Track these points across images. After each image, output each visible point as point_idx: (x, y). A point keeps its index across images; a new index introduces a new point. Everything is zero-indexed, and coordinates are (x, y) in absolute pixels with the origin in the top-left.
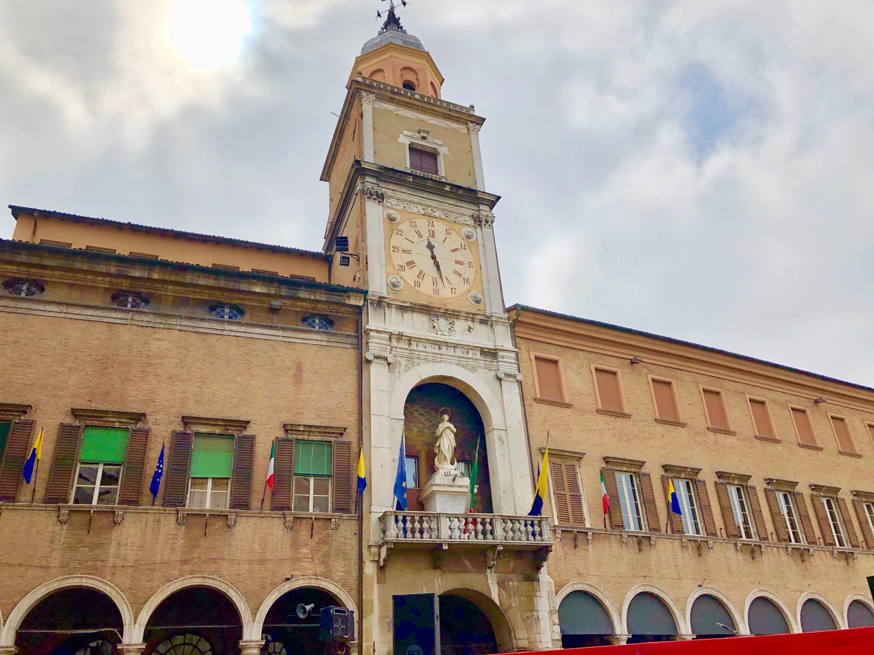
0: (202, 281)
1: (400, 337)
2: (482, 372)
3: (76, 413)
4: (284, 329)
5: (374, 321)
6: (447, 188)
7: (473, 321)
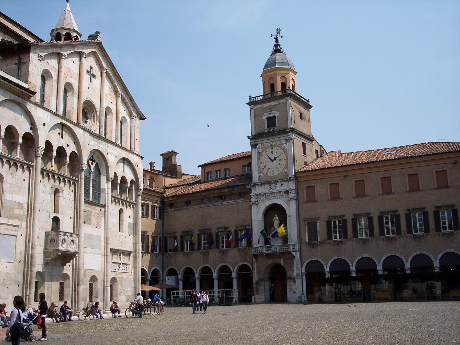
0: (215, 192)
2: (285, 199)
3: (200, 231)
4: (235, 199)
5: (253, 192)
6: (276, 133)
7: (283, 181)
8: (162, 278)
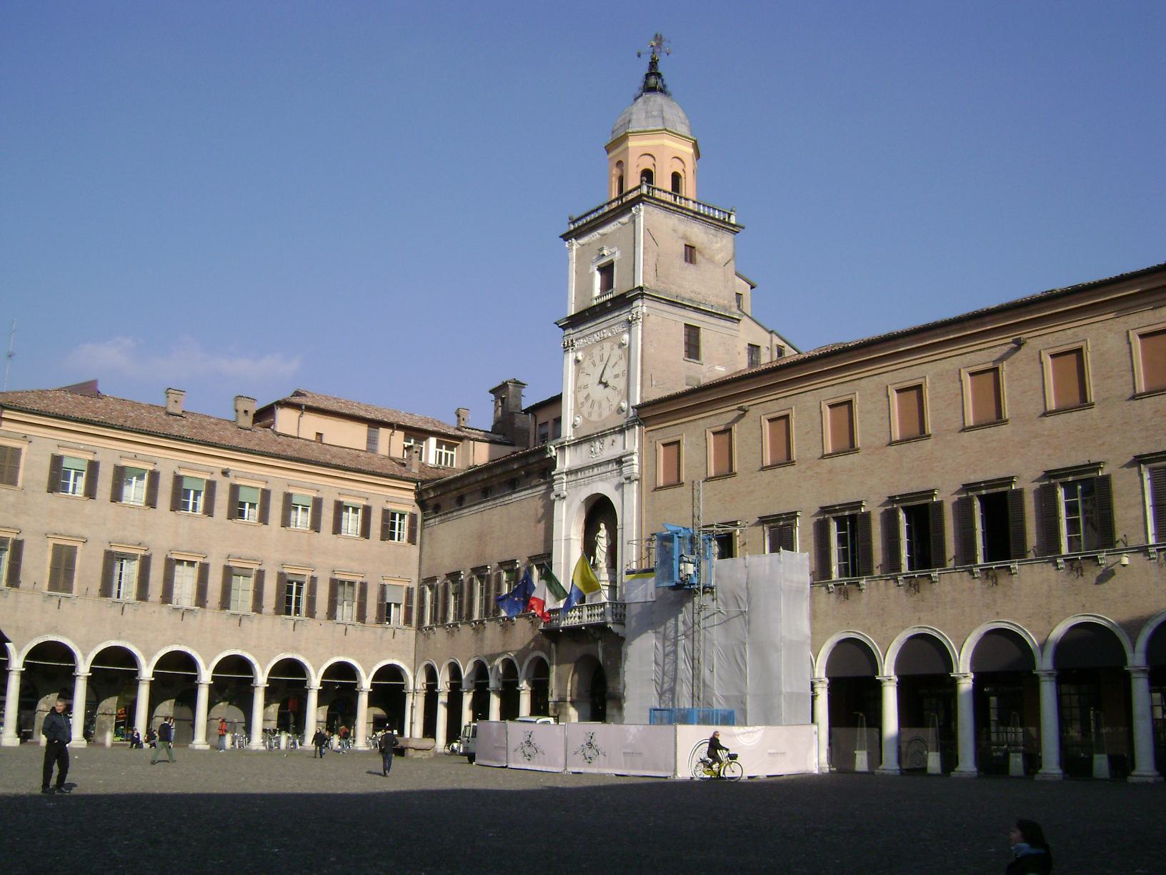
0: (499, 471)
8: (411, 687)
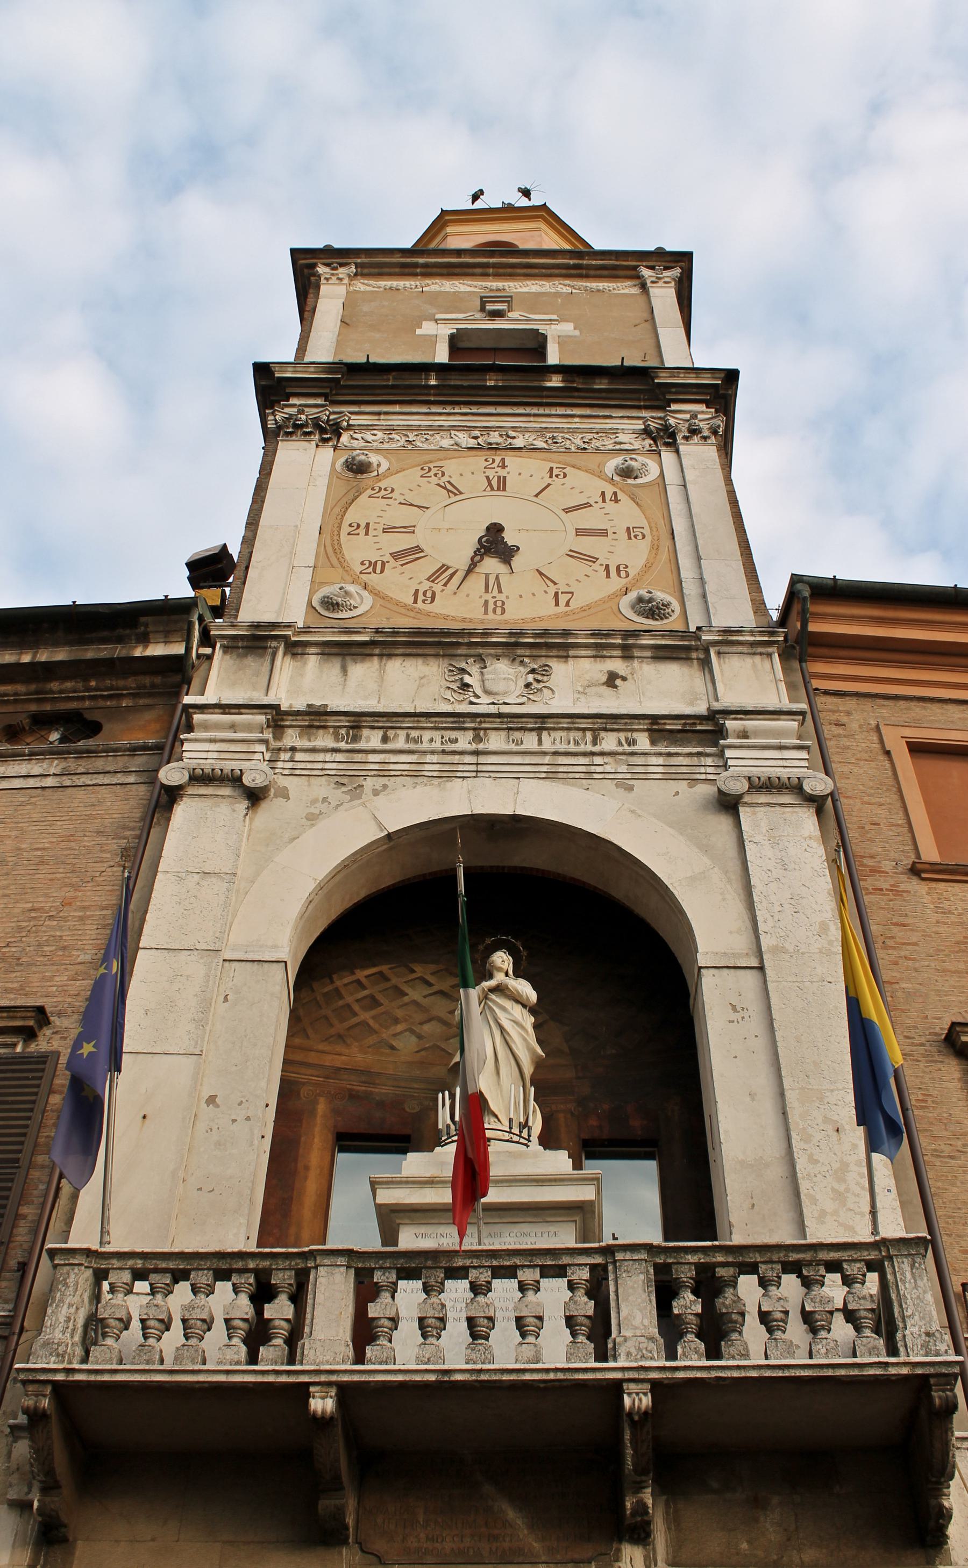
1: (316, 718)
